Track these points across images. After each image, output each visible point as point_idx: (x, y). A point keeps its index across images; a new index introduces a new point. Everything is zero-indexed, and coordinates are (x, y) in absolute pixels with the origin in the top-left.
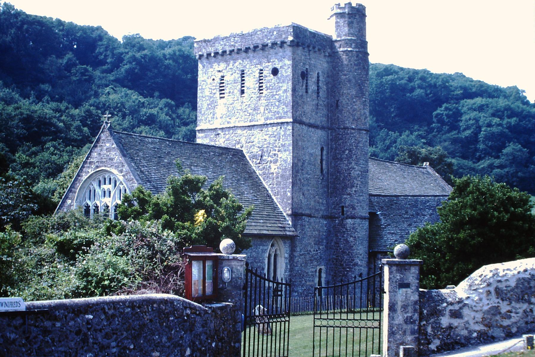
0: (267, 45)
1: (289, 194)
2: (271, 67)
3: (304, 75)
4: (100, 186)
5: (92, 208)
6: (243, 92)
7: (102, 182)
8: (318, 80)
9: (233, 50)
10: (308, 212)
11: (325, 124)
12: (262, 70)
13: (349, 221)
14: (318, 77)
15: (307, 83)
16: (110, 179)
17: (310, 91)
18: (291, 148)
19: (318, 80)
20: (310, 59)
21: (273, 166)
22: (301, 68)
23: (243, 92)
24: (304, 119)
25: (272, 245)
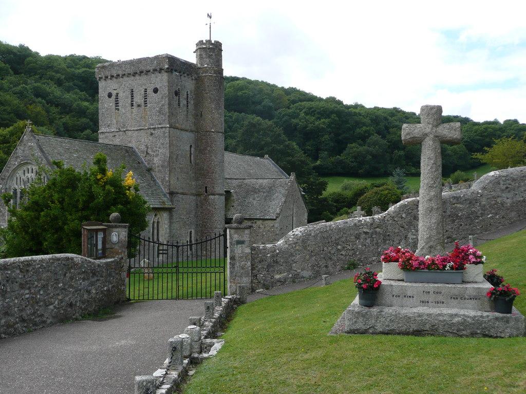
0: (149, 71)
1: (167, 179)
3: (177, 93)
4: (24, 174)
5: (19, 191)
6: (132, 105)
7: (26, 172)
8: (187, 97)
9: (125, 75)
11: (193, 128)
14: (187, 95)
16: (32, 169)
17: (181, 105)
18: (168, 145)
21: (156, 159)
22: (175, 88)
23: (132, 105)
24: (177, 125)
25: (156, 215)
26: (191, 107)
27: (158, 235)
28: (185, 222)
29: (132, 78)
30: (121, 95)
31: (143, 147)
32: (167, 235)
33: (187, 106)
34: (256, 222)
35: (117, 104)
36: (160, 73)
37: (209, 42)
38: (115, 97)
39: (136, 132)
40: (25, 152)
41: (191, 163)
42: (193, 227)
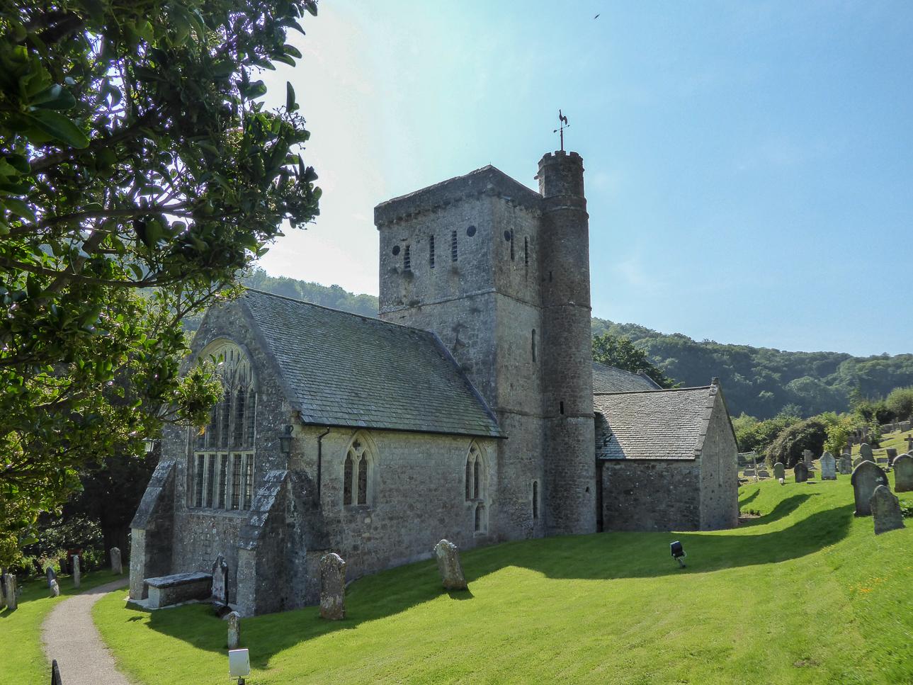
2: (466, 226)
3: (509, 236)
6: (432, 262)
8: (526, 246)
10: (517, 408)
12: (455, 232)
13: (573, 420)
15: (512, 247)
17: (517, 257)
19: (526, 246)
20: (515, 217)
21: (472, 351)
23: (432, 262)
24: (510, 291)
25: (472, 450)
26: (533, 264)
27: (476, 487)
28: (525, 465)
29: (432, 216)
30: (413, 247)
31: (448, 332)
32: (494, 488)
33: (527, 262)
34: (654, 467)
35: (407, 263)
36: (478, 199)
37: (561, 154)
38: (404, 253)
39: (439, 307)
40: (220, 320)
41: (534, 360)
42: (539, 474)
